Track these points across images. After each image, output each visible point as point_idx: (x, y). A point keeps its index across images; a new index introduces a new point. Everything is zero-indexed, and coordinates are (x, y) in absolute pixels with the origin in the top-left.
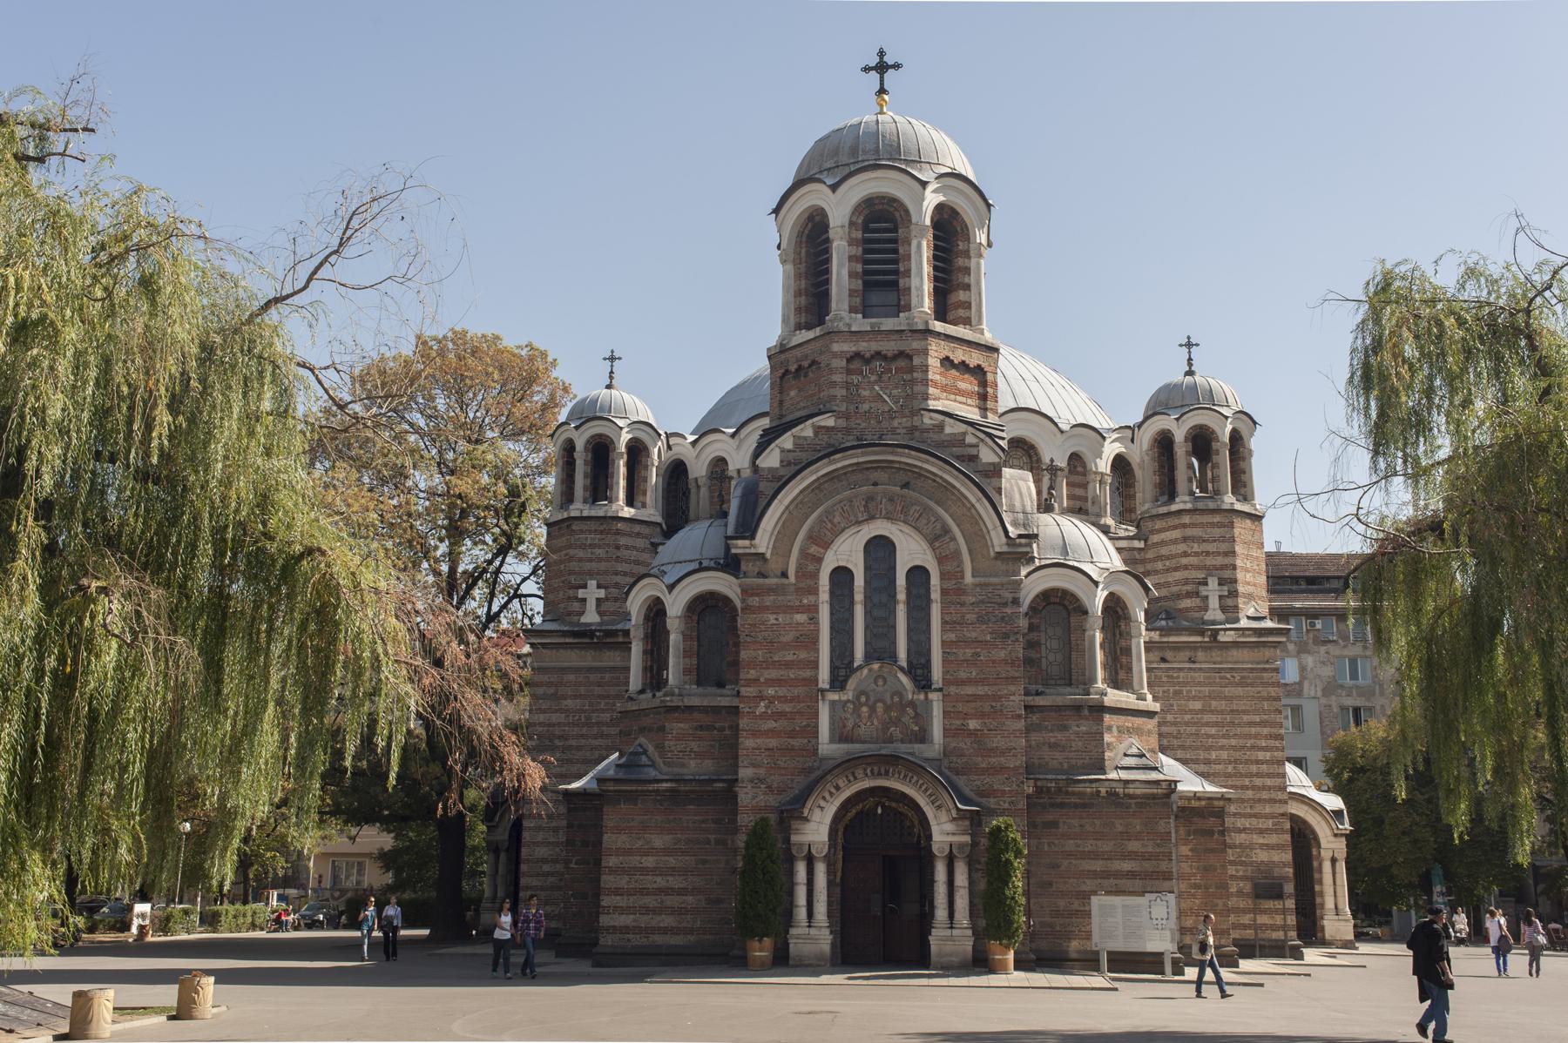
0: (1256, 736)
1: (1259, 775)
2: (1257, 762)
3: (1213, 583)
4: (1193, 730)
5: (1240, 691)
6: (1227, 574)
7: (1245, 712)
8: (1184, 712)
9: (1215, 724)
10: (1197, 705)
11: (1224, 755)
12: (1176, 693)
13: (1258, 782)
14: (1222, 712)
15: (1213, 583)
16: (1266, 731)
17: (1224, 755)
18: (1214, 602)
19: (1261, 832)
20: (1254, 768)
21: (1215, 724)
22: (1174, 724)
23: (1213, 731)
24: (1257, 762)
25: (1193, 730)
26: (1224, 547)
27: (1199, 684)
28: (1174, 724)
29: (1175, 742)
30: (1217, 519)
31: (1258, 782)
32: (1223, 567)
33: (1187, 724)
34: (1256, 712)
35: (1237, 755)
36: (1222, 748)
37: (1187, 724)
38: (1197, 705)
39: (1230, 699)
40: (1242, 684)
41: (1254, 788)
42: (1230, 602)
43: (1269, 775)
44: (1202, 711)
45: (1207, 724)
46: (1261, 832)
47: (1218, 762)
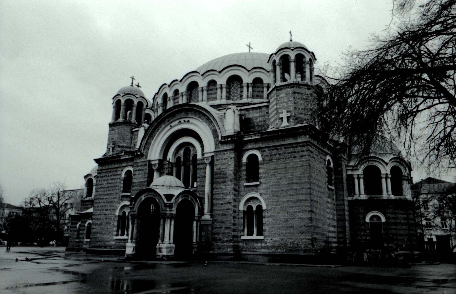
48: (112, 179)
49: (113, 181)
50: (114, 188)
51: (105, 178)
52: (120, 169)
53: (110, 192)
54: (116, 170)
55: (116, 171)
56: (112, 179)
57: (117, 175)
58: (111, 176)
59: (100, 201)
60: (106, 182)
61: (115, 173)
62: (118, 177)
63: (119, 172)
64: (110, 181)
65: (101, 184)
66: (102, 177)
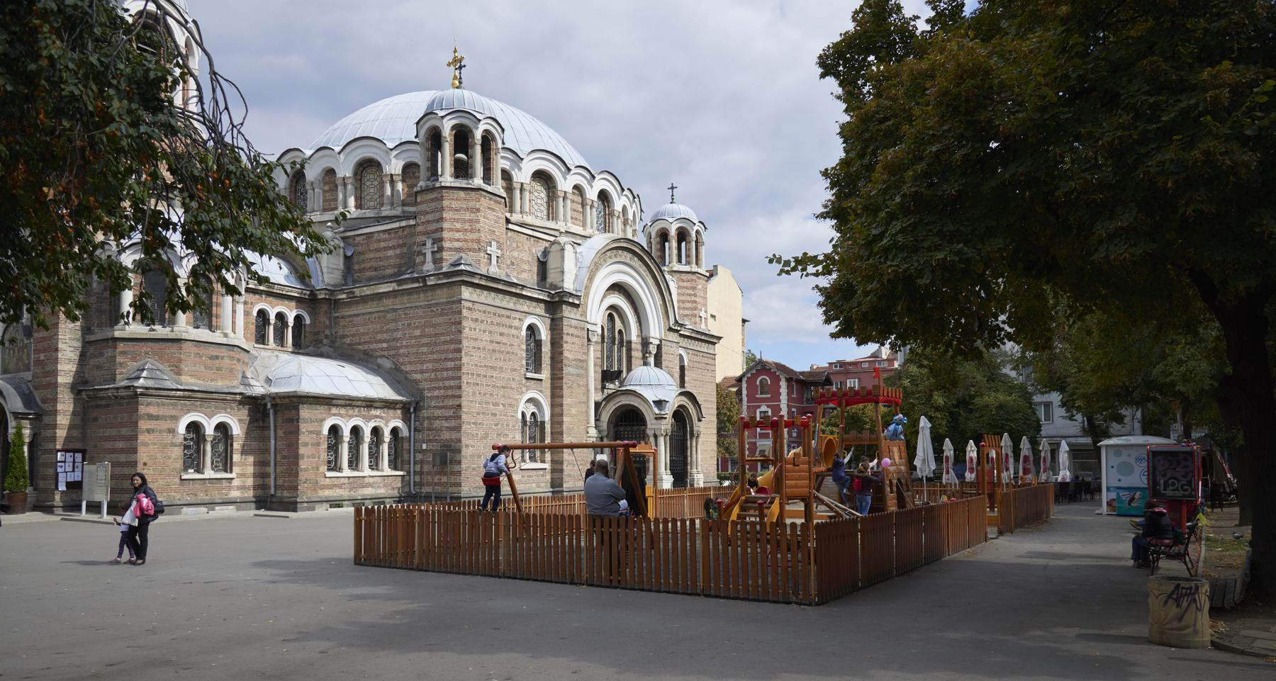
0: (447, 351)
1: (448, 379)
2: (447, 369)
3: (429, 244)
4: (415, 350)
5: (440, 320)
6: (436, 235)
7: (442, 334)
8: (411, 338)
9: (427, 345)
10: (417, 332)
11: (430, 366)
12: (409, 325)
13: (447, 383)
14: (430, 336)
15: (429, 244)
16: (452, 347)
17: (430, 366)
18: (429, 257)
19: (447, 418)
20: (445, 374)
21: (427, 345)
22: (407, 347)
23: (425, 350)
24: (447, 369)
25: (415, 350)
26: (437, 215)
27: (420, 317)
28: (407, 347)
29: (407, 360)
30: (434, 195)
31: (447, 383)
32: (437, 230)
33: (413, 346)
34: (447, 334)
35: (437, 365)
36: (429, 361)
37: (413, 346)
38: (417, 332)
39: (434, 326)
40: (442, 315)
41: (445, 388)
42: (438, 256)
43: (453, 378)
44: (420, 337)
45: (423, 345)
46: (447, 418)
47: (427, 371)
48: (501, 334)
49: (504, 340)
50: (507, 357)
51: (483, 327)
52: (517, 315)
53: (500, 364)
54: (508, 313)
55: (508, 317)
56: (501, 334)
57: (511, 327)
58: (498, 324)
59: (478, 380)
60: (486, 337)
61: (505, 320)
62: (514, 332)
63: (516, 323)
64: (499, 338)
65: (476, 340)
66: (477, 320)
